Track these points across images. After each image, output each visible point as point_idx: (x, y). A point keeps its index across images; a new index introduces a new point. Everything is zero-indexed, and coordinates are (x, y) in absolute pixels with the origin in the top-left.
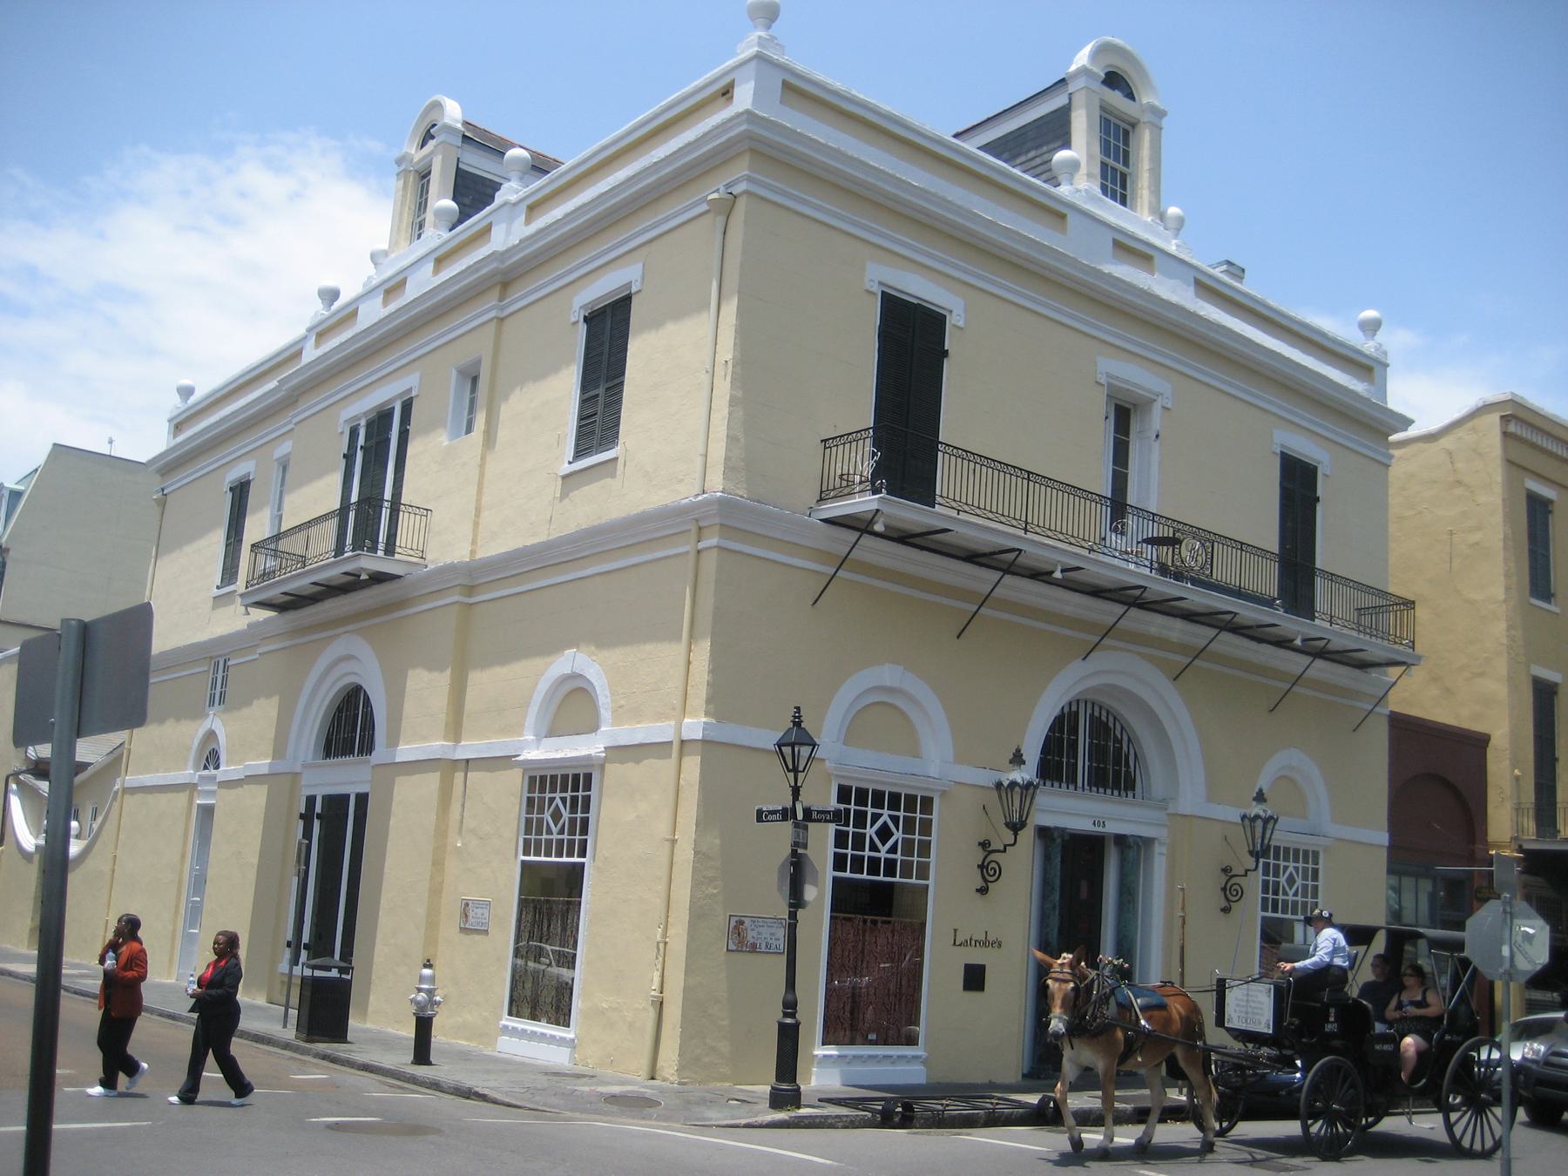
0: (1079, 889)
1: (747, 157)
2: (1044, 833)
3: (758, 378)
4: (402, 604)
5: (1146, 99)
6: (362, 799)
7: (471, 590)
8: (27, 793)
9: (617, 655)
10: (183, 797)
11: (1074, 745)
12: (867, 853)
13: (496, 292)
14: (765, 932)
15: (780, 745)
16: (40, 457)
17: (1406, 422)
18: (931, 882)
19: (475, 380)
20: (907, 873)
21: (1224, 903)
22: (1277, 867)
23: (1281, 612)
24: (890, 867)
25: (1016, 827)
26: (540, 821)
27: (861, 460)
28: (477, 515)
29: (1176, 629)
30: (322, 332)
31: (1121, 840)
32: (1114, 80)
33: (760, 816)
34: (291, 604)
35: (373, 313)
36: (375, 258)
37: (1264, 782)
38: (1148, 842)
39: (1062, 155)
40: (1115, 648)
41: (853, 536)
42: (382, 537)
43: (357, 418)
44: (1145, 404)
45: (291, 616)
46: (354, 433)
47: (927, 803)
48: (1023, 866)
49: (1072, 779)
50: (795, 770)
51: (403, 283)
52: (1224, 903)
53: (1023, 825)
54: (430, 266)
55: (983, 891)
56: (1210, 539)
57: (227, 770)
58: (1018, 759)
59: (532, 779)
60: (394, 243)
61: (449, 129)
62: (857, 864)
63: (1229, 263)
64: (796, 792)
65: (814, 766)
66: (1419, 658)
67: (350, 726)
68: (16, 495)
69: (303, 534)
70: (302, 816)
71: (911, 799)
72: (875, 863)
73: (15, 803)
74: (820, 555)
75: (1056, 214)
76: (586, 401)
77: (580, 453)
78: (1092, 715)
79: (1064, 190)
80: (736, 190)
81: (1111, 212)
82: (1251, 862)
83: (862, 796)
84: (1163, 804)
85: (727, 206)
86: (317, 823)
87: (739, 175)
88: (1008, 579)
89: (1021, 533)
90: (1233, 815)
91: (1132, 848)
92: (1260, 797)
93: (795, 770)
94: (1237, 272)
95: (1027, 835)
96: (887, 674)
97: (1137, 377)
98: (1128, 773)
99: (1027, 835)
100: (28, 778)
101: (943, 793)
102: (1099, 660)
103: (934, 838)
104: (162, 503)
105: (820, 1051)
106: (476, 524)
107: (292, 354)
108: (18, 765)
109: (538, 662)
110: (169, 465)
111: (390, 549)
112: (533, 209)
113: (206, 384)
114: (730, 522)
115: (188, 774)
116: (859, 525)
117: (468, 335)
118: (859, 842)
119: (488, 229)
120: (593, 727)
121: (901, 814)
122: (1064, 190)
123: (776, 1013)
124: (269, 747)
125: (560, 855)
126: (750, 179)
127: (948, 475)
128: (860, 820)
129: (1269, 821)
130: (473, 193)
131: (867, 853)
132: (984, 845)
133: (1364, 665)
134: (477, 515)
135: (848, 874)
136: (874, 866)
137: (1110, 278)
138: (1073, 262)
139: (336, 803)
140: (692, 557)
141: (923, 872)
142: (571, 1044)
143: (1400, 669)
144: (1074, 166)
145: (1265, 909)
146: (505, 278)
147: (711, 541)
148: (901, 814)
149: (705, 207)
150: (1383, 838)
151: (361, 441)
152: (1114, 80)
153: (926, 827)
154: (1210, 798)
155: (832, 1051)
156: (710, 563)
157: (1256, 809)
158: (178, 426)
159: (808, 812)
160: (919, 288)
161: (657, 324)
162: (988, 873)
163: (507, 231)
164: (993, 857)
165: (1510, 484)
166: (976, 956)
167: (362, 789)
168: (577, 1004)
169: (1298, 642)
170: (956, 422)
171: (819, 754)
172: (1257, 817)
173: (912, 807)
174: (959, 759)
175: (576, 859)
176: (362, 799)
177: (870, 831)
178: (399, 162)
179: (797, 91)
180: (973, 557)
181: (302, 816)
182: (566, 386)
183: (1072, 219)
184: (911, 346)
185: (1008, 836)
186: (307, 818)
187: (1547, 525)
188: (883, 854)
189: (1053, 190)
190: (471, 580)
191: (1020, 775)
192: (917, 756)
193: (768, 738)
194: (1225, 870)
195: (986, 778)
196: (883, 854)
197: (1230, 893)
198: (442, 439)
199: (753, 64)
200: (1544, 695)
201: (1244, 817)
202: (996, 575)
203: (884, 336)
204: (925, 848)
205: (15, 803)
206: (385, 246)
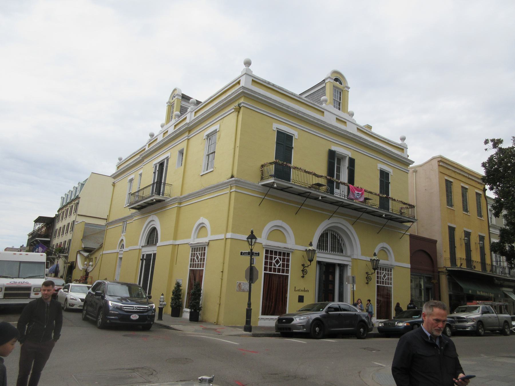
0: (329, 278)
2: (319, 263)
6: (155, 255)
15: (248, 238)
18: (289, 274)
19: (183, 154)
20: (283, 272)
21: (366, 282)
22: (380, 273)
24: (279, 271)
25: (311, 261)
26: (194, 259)
31: (339, 265)
32: (336, 80)
34: (140, 208)
35: (160, 138)
36: (162, 126)
37: (376, 251)
38: (347, 265)
39: (323, 98)
41: (268, 188)
42: (161, 192)
43: (156, 164)
46: (156, 167)
47: (288, 255)
48: (313, 271)
50: (251, 245)
52: (366, 282)
53: (312, 260)
55: (303, 277)
57: (125, 249)
58: (311, 245)
59: (192, 248)
62: (270, 270)
65: (256, 244)
66: (417, 220)
67: (152, 237)
69: (142, 191)
70: (141, 259)
71: (284, 254)
72: (275, 269)
74: (261, 193)
79: (324, 105)
82: (373, 271)
83: (271, 252)
86: (144, 261)
88: (308, 200)
90: (368, 259)
91: (342, 267)
92: (375, 255)
93: (251, 245)
94: (370, 127)
95: (314, 263)
96: (279, 222)
98: (341, 248)
99: (314, 263)
102: (333, 220)
103: (290, 263)
104: (114, 184)
105: (261, 316)
110: (115, 176)
111: (163, 195)
115: (117, 250)
116: (270, 186)
117: (181, 144)
118: (271, 264)
119: (186, 118)
120: (206, 236)
121: (282, 257)
122: (324, 105)
123: (246, 307)
125: (198, 267)
127: (293, 174)
129: (378, 260)
130: (183, 110)
132: (303, 265)
135: (268, 272)
138: (325, 123)
139: (149, 256)
140: (228, 194)
143: (411, 223)
144: (326, 101)
145: (378, 283)
146: (189, 129)
147: (233, 190)
148: (282, 257)
149: (233, 110)
150: (409, 266)
151: (157, 169)
153: (288, 260)
154: (362, 255)
156: (233, 195)
157: (374, 258)
158: (118, 167)
162: (304, 272)
163: (190, 117)
164: (305, 268)
165: (440, 178)
166: (302, 294)
167: (155, 252)
169: (384, 216)
170: (296, 160)
171: (258, 241)
172: (374, 259)
173: (285, 255)
174: (296, 244)
175: (201, 268)
176: (155, 255)
177: (274, 261)
179: (256, 81)
181: (141, 259)
183: (325, 112)
184: (284, 142)
185: (309, 263)
186: (142, 260)
187: (451, 188)
189: (320, 106)
190: (180, 201)
191: (311, 248)
193: (245, 237)
194: (367, 273)
195: (303, 248)
197: (368, 279)
199: (245, 76)
200: (452, 230)
201: (371, 260)
202: (305, 199)
204: (288, 266)
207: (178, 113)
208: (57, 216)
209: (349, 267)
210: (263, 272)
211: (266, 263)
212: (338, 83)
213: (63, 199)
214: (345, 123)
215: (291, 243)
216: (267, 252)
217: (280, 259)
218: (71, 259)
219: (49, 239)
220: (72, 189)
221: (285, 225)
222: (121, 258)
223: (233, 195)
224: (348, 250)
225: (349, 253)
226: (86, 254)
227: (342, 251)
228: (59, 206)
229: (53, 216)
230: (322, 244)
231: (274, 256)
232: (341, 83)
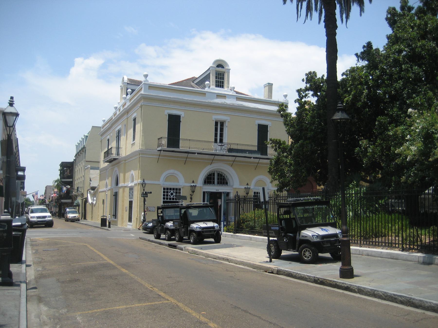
1: (143, 100)
4: (119, 163)
7: (125, 160)
8: (90, 193)
10: (104, 193)
11: (214, 179)
14: (152, 209)
16: (90, 129)
27: (165, 142)
29: (230, 158)
30: (115, 114)
32: (219, 66)
39: (207, 82)
40: (214, 163)
44: (225, 121)
47: (180, 189)
49: (214, 183)
56: (230, 144)
62: (167, 199)
64: (144, 190)
68: (87, 136)
71: (177, 189)
75: (204, 94)
79: (207, 89)
81: (219, 91)
83: (167, 189)
84: (232, 186)
85: (141, 107)
87: (142, 102)
90: (243, 187)
96: (171, 171)
100: (90, 190)
101: (182, 188)
102: (213, 165)
104: (101, 141)
108: (89, 188)
113: (107, 118)
114: (141, 153)
116: (160, 150)
118: (167, 195)
122: (207, 89)
128: (167, 192)
132: (191, 195)
136: (170, 199)
137: (215, 103)
139: (116, 193)
152: (219, 66)
159: (146, 193)
160: (175, 112)
173: (177, 190)
182: (132, 130)
184: (174, 122)
188: (172, 197)
191: (192, 185)
195: (189, 185)
196: (172, 197)
205: (89, 195)
206: (119, 101)
208: (75, 160)
211: (164, 195)
212: (220, 68)
214: (225, 96)
215: (182, 183)
216: (164, 189)
217: (174, 192)
219: (71, 180)
221: (176, 172)
224: (230, 182)
226: (92, 191)
228: (75, 153)
230: (209, 180)
232: (223, 67)
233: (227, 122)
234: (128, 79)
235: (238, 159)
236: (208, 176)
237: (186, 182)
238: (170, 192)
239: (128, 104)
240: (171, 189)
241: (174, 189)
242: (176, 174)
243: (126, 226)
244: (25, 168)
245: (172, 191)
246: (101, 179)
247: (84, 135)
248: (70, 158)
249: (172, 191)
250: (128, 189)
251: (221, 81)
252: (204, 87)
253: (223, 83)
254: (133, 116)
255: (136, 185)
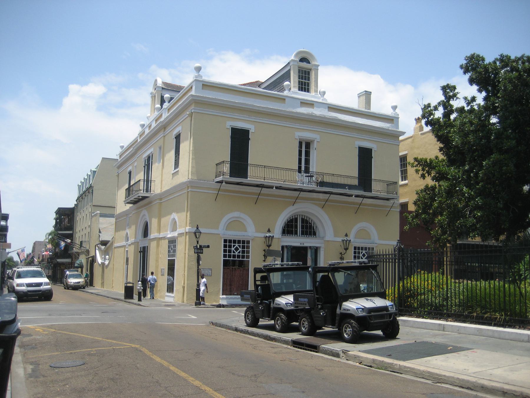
1: (194, 104)
3: (198, 154)
4: (150, 203)
5: (314, 63)
7: (161, 199)
8: (100, 249)
9: (179, 214)
11: (296, 227)
12: (232, 254)
13: (163, 130)
14: (206, 272)
16: (99, 162)
17: (403, 133)
18: (250, 259)
23: (348, 190)
24: (239, 256)
27: (226, 168)
28: (162, 182)
29: (321, 196)
30: (141, 135)
32: (303, 60)
33: (208, 247)
38: (320, 247)
39: (287, 83)
44: (313, 141)
45: (136, 205)
47: (248, 242)
51: (151, 125)
54: (154, 122)
56: (323, 174)
60: (151, 114)
61: (159, 87)
62: (230, 256)
63: (366, 91)
64: (198, 243)
68: (94, 172)
71: (244, 242)
73: (97, 252)
75: (283, 99)
76: (176, 157)
77: (175, 169)
78: (302, 218)
79: (286, 93)
80: (192, 111)
81: (303, 96)
83: (230, 241)
85: (191, 115)
89: (263, 180)
90: (340, 239)
91: (316, 250)
96: (236, 214)
97: (307, 135)
101: (252, 240)
102: (296, 206)
104: (118, 176)
105: (221, 296)
106: (161, 184)
107: (135, 141)
108: (98, 242)
109: (169, 216)
112: (169, 110)
113: (126, 144)
116: (221, 182)
118: (230, 251)
122: (286, 93)
124: (134, 236)
126: (194, 109)
128: (230, 246)
131: (232, 254)
133: (388, 199)
134: (162, 182)
136: (234, 256)
139: (144, 248)
140: (187, 193)
141: (248, 257)
142: (173, 297)
147: (189, 190)
152: (303, 60)
154: (335, 236)
155: (224, 296)
159: (200, 246)
161: (183, 142)
168: (175, 289)
173: (245, 244)
174: (256, 232)
178: (151, 94)
180: (257, 186)
182: (173, 152)
184: (240, 140)
188: (236, 253)
191: (268, 235)
192: (246, 231)
194: (341, 253)
195: (263, 235)
196: (236, 253)
198: (157, 164)
203: (232, 138)
205: (97, 252)
206: (149, 115)
207: (159, 106)
208: (76, 205)
209: (321, 249)
210: (222, 258)
211: (225, 251)
212: (305, 63)
213: (79, 187)
214: (313, 104)
215: (251, 231)
216: (225, 241)
218: (92, 254)
219: (71, 232)
220: (86, 177)
221: (243, 216)
222: (127, 251)
223: (189, 193)
225: (322, 235)
226: (103, 247)
227: (315, 234)
228: (76, 195)
229: (72, 206)
230: (289, 228)
231: (232, 244)
232: (309, 63)
233: (315, 142)
234: (163, 83)
235: (333, 197)
236: (288, 222)
237: (257, 231)
238: (234, 246)
239: (165, 115)
240: (235, 242)
241: (239, 242)
242: (242, 219)
243: (164, 298)
244: (8, 215)
245: (237, 245)
246: (117, 229)
247: (91, 170)
248: (70, 203)
249: (237, 245)
250: (167, 241)
251: (305, 83)
252: (282, 90)
253: (308, 85)
254: (175, 132)
255: (181, 235)
